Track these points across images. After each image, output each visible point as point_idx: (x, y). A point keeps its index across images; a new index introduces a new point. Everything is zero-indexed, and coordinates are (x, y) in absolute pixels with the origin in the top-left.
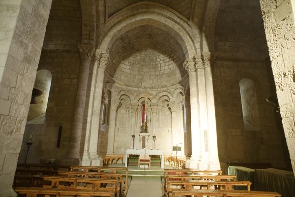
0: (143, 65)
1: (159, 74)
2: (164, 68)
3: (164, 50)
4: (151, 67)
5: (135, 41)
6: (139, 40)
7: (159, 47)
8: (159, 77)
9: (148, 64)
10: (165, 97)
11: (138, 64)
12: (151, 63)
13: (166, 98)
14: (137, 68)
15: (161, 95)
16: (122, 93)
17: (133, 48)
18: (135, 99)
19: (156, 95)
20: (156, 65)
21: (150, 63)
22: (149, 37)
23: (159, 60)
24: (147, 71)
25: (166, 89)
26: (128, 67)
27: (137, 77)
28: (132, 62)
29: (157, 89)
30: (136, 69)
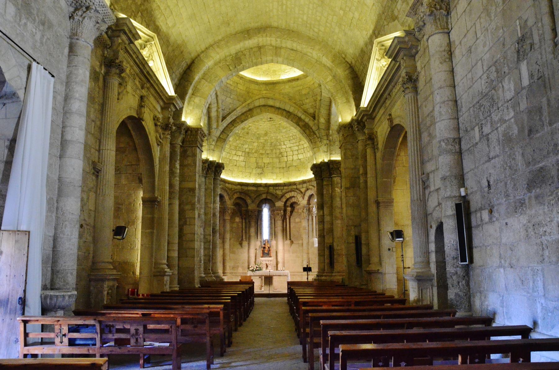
0: (262, 154)
1: (285, 166)
2: (291, 157)
3: (291, 135)
4: (274, 156)
5: (250, 125)
6: (257, 123)
7: (284, 131)
8: (285, 169)
9: (268, 152)
10: (293, 199)
11: (255, 153)
12: (274, 151)
13: (293, 200)
14: (255, 159)
15: (288, 196)
16: (236, 196)
17: (248, 133)
18: (253, 202)
19: (282, 197)
20: (281, 153)
21: (272, 150)
22: (269, 120)
23: (284, 147)
24: (268, 161)
25: (295, 187)
26: (242, 158)
27: (254, 171)
28: (247, 150)
29: (282, 188)
30: (253, 160)
